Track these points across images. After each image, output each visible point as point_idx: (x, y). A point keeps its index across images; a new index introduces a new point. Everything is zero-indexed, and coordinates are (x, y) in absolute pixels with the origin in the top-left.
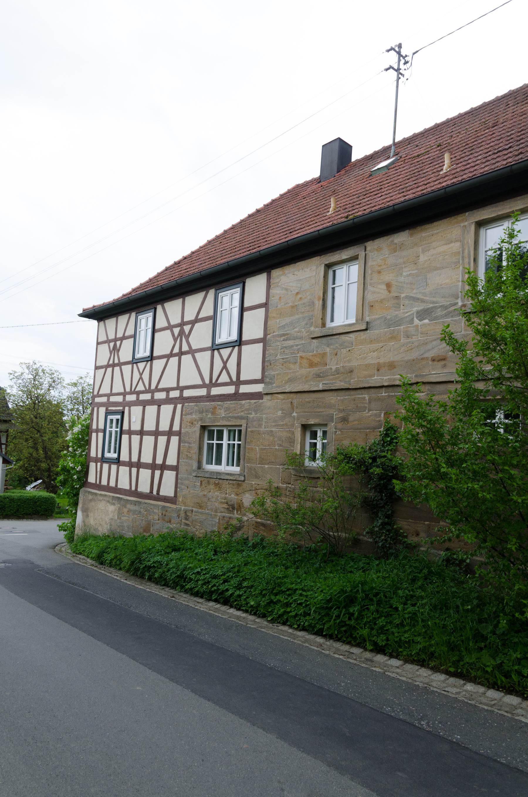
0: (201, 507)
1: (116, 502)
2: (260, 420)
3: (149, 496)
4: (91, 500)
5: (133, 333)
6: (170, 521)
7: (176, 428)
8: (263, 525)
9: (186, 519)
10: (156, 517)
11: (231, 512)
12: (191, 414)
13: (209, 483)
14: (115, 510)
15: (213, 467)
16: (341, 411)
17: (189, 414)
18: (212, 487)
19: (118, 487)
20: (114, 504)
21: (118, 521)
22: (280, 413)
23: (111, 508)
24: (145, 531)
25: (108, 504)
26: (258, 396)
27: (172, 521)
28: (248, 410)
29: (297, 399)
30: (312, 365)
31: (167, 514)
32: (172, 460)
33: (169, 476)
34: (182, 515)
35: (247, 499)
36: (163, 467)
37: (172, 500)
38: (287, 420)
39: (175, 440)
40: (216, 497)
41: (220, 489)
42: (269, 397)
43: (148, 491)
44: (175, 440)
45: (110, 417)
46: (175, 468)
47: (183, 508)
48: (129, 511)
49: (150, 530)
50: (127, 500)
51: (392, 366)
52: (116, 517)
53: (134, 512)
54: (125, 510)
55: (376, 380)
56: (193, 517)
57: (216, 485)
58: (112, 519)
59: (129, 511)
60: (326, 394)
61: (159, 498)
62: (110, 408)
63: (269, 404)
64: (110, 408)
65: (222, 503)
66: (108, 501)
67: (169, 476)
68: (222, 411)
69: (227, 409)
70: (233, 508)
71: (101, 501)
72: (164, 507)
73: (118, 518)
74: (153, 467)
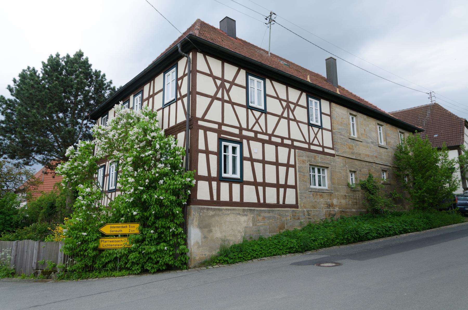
0: (315, 208)
1: (249, 213)
2: (335, 166)
3: (277, 205)
4: (213, 216)
5: (118, 79)
6: (299, 219)
7: (292, 162)
8: (343, 211)
9: (309, 215)
10: (289, 218)
11: (329, 208)
12: (303, 156)
13: (317, 195)
14: (249, 219)
15: (312, 186)
16: (360, 167)
17: (301, 156)
18: (319, 196)
19: (233, 200)
20: (246, 215)
21: (254, 227)
22: (342, 164)
23: (245, 218)
24: (280, 229)
25: (239, 216)
26: (333, 155)
27: (300, 218)
28: (331, 161)
29: (347, 160)
30: (350, 148)
31: (296, 215)
32: (291, 182)
33: (291, 193)
34: (306, 213)
35: (335, 202)
36: (286, 186)
37: (296, 206)
38: (345, 168)
39: (291, 170)
40: (322, 201)
41: (323, 197)
42: (338, 157)
43: (275, 202)
44: (291, 170)
45: (224, 143)
46: (295, 187)
47: (305, 210)
48: (264, 218)
49: (284, 228)
50: (261, 210)
51: (368, 156)
52: (251, 225)
53: (269, 218)
54: (260, 218)
55: (366, 159)
56: (312, 214)
57: (321, 195)
58: (246, 227)
59: (264, 218)
60: (355, 161)
61: (265, 205)
62: (222, 135)
63: (338, 160)
64: (222, 135)
65: (324, 204)
66: (239, 214)
67: (291, 193)
68: (319, 159)
69: (321, 158)
70: (330, 206)
71: (229, 214)
72: (293, 211)
73: (253, 225)
74: (277, 186)
